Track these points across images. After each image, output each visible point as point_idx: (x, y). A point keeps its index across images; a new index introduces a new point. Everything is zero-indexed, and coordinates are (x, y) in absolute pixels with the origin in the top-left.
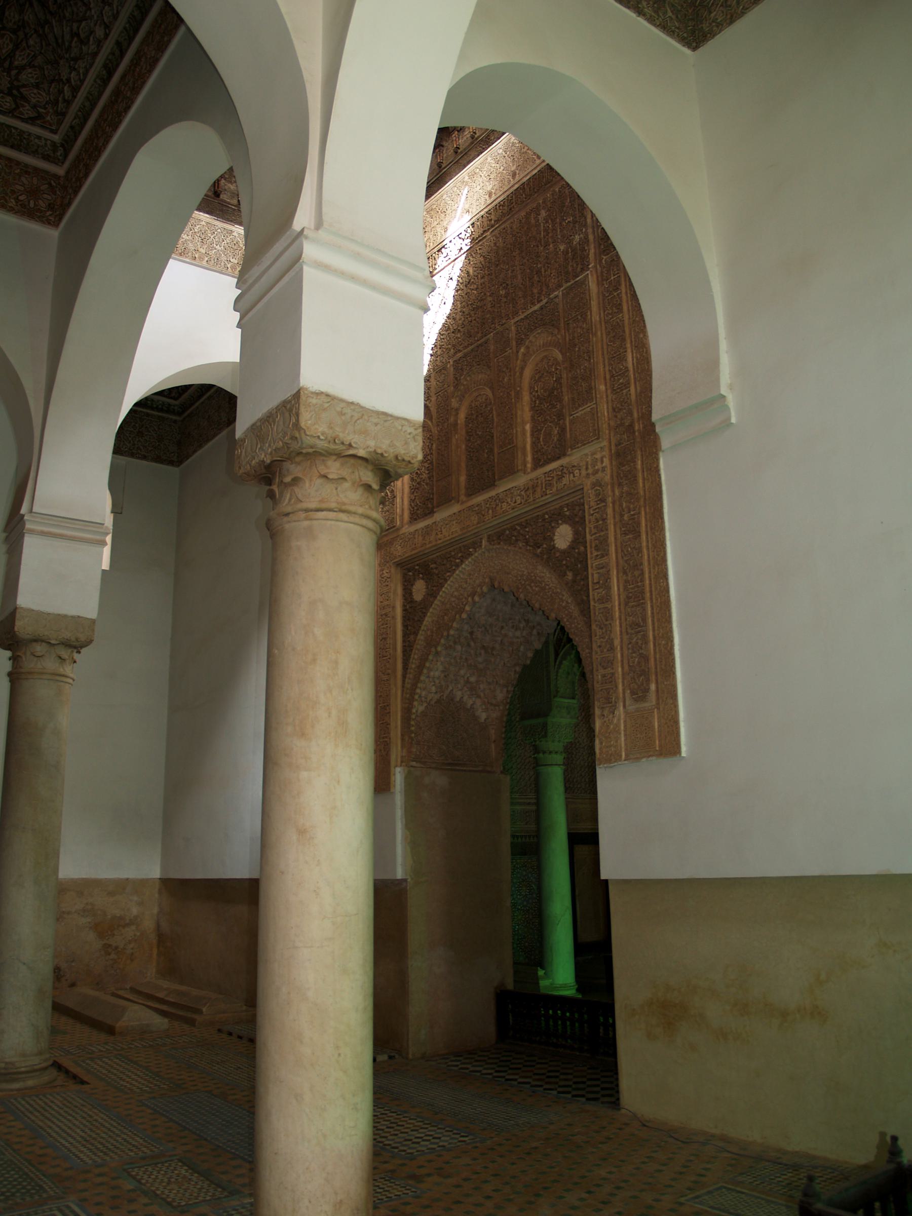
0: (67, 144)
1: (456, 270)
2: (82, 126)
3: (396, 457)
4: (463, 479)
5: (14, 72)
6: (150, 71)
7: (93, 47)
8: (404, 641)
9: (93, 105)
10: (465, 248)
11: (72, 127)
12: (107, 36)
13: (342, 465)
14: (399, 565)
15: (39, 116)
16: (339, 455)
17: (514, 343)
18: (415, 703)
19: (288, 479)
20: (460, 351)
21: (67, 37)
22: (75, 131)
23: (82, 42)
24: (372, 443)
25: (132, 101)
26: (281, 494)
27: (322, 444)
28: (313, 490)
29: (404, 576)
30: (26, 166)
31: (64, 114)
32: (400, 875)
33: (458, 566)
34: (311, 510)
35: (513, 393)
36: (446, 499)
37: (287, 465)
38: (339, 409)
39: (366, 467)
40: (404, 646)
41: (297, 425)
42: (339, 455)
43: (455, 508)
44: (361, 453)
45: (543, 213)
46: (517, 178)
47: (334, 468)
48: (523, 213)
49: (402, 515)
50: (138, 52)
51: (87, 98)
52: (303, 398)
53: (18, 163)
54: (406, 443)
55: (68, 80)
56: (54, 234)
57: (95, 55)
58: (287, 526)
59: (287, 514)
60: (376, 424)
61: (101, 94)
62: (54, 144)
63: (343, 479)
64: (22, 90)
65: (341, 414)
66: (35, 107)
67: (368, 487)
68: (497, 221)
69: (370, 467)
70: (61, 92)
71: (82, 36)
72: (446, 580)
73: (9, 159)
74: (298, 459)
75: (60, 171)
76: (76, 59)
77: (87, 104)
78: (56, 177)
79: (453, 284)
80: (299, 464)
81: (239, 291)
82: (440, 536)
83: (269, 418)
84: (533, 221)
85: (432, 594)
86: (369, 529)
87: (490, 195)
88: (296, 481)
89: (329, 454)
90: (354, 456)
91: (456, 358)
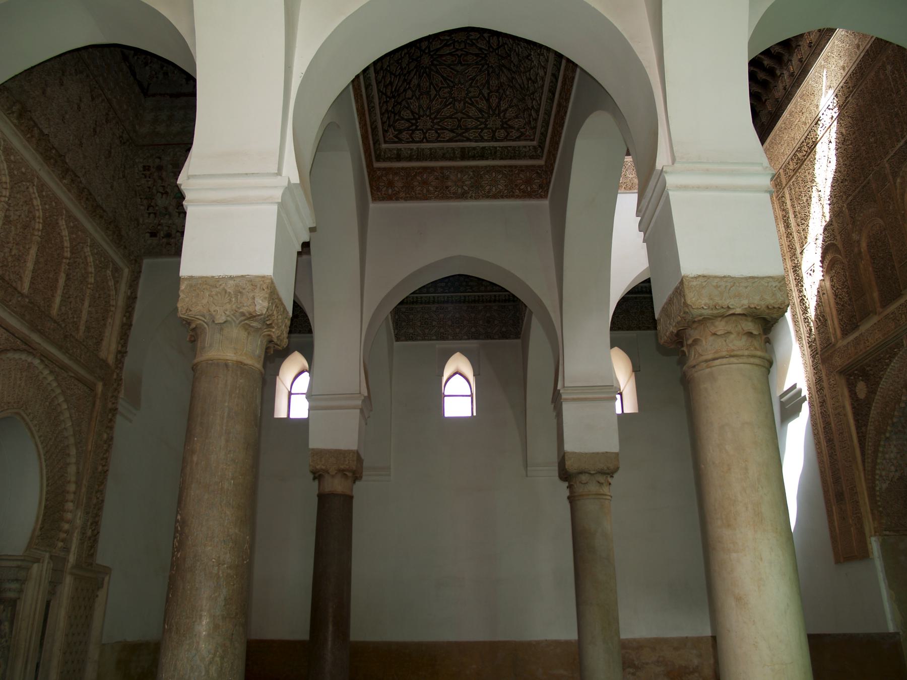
0: (541, 145)
1: (833, 134)
2: (547, 131)
3: (768, 307)
4: (876, 295)
5: (502, 115)
6: (572, 86)
7: (540, 82)
8: (858, 433)
9: (549, 116)
10: (835, 116)
11: (542, 134)
12: (545, 73)
13: (727, 322)
14: (841, 372)
15: (522, 134)
16: (723, 316)
17: (891, 177)
18: (877, 482)
19: (690, 342)
20: (850, 195)
21: (525, 83)
22: (544, 134)
23: (534, 82)
24: (745, 302)
25: (567, 107)
26: (689, 352)
27: (707, 312)
28: (708, 346)
29: (848, 380)
30: (521, 167)
31: (535, 128)
32: (891, 628)
33: (888, 365)
34: (710, 360)
35: (899, 217)
36: (865, 314)
37: (690, 332)
38: (714, 284)
39: (746, 320)
40: (859, 437)
41: (685, 303)
42: (723, 316)
43: (875, 319)
44: (739, 311)
45: (889, 67)
46: (861, 48)
47: (721, 326)
48: (873, 74)
49: (835, 334)
50: (564, 75)
51: (545, 113)
52: (686, 283)
53: (516, 167)
54: (774, 294)
55: (533, 107)
56: (545, 203)
57: (543, 86)
58: (696, 375)
59: (694, 367)
60: (746, 287)
61: (551, 108)
62: (534, 147)
63: (729, 333)
64: (509, 123)
65: (717, 287)
66: (518, 130)
67: (750, 334)
68: (854, 87)
69: (750, 319)
70: (530, 115)
71: (533, 78)
72: (881, 378)
73: (511, 167)
74: (695, 325)
75: (541, 162)
76: (533, 93)
77: (546, 117)
78: (540, 167)
79: (833, 146)
80: (696, 329)
81: (639, 218)
82: (867, 344)
83: (670, 301)
84: (882, 77)
85: (872, 392)
86: (757, 365)
87: (844, 68)
88: (696, 341)
89: (715, 317)
90: (733, 314)
91: (848, 202)
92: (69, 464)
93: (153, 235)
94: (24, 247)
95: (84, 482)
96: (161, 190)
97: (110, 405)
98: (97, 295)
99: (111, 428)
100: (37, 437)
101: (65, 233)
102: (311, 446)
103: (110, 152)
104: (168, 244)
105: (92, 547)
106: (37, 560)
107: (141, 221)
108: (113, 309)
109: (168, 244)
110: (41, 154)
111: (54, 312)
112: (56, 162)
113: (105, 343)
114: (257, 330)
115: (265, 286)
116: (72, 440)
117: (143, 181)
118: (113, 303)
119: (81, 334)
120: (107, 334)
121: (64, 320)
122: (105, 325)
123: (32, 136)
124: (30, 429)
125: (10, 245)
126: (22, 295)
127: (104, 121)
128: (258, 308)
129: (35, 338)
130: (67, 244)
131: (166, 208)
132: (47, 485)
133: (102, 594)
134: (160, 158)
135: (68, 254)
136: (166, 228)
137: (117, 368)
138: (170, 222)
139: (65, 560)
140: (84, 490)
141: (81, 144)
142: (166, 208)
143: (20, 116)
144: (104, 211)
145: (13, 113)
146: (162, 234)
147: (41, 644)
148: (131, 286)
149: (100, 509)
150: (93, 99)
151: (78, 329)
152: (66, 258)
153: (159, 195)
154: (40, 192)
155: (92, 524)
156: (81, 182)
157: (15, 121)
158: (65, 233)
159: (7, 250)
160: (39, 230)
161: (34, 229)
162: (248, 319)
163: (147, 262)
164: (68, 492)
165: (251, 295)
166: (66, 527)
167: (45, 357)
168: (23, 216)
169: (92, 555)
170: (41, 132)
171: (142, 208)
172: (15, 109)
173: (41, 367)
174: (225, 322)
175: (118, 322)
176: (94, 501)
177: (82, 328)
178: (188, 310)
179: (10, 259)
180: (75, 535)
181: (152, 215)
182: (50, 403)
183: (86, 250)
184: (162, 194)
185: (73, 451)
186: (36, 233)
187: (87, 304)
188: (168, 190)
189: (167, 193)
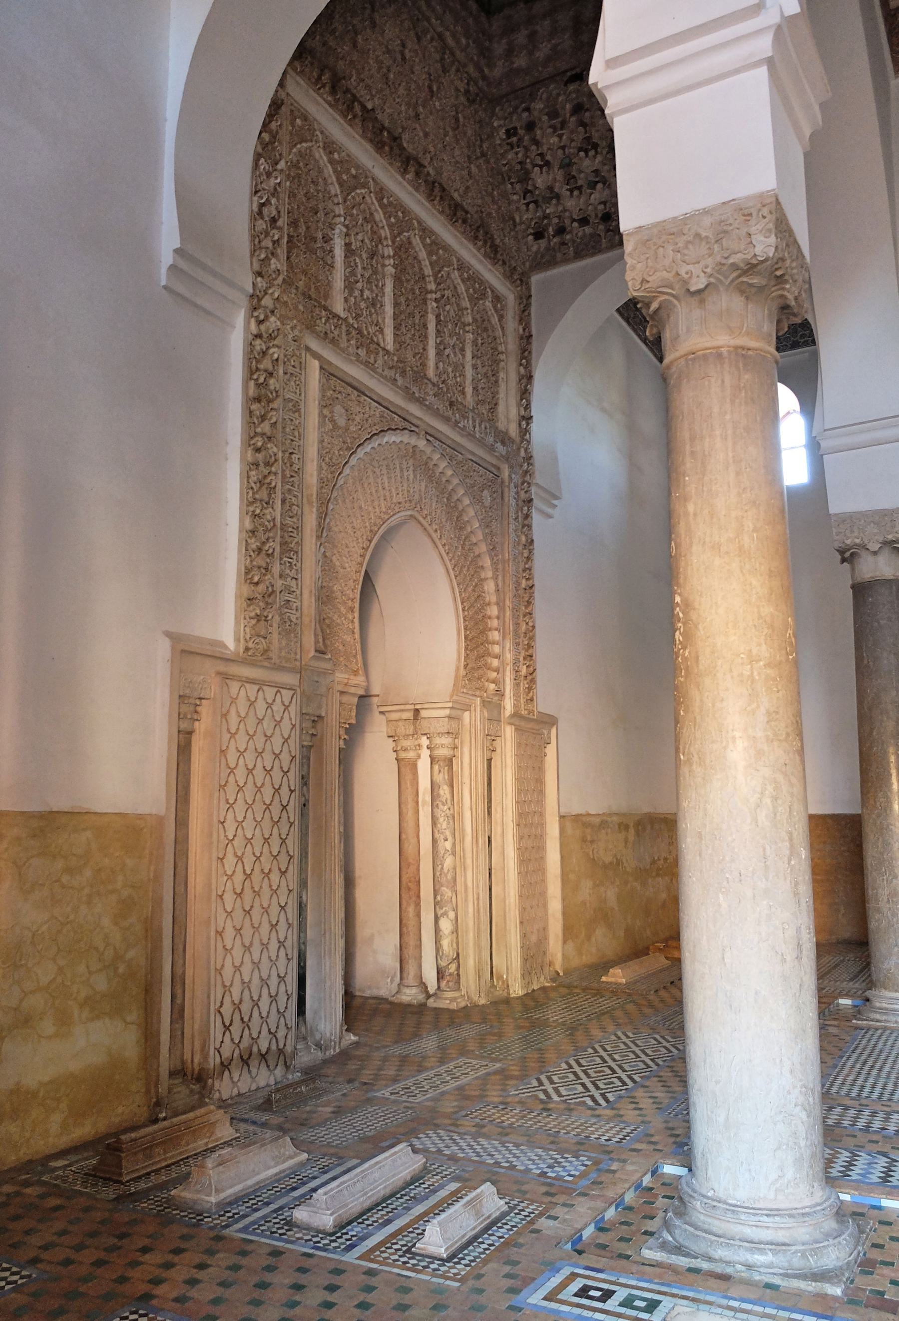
92: (482, 580)
94: (377, 286)
95: (508, 603)
97: (523, 495)
98: (480, 341)
99: (530, 527)
100: (440, 547)
101: (423, 255)
102: (833, 510)
103: (457, 120)
104: (564, 244)
105: (530, 689)
106: (467, 708)
107: (518, 220)
108: (502, 357)
109: (564, 244)
110: (371, 141)
111: (431, 373)
112: (391, 148)
113: (501, 408)
114: (761, 289)
115: (765, 212)
116: (483, 548)
118: (501, 348)
119: (469, 399)
120: (502, 395)
121: (443, 382)
122: (497, 382)
123: (355, 117)
124: (430, 536)
125: (359, 285)
126: (388, 352)
127: (440, 72)
128: (759, 250)
129: (414, 410)
130: (428, 271)
131: (550, 188)
132: (463, 610)
133: (551, 750)
134: (527, 109)
135: (432, 286)
136: (555, 221)
137: (522, 440)
138: (560, 208)
139: (499, 707)
140: (508, 613)
141: (417, 116)
142: (550, 188)
143: (333, 90)
144: (467, 212)
145: (324, 86)
147: (489, 813)
148: (521, 320)
149: (532, 638)
150: (419, 39)
151: (463, 393)
152: (431, 292)
154: (380, 200)
155: (525, 659)
156: (428, 173)
157: (329, 98)
158: (423, 255)
159: (357, 293)
160: (389, 257)
161: (383, 257)
162: (745, 273)
163: (536, 279)
164: (490, 618)
165: (744, 231)
166: (495, 663)
167: (431, 436)
168: (366, 241)
169: (532, 700)
170: (364, 107)
171: (515, 197)
172: (325, 78)
173: (428, 450)
174: (706, 287)
175: (513, 377)
176: (524, 627)
177: (469, 390)
178: (644, 281)
179: (363, 305)
180: (508, 673)
181: (532, 206)
182: (448, 499)
183: (453, 276)
184: (541, 167)
185: (487, 562)
186: (387, 262)
187: (469, 355)
188: (548, 158)
189: (547, 164)
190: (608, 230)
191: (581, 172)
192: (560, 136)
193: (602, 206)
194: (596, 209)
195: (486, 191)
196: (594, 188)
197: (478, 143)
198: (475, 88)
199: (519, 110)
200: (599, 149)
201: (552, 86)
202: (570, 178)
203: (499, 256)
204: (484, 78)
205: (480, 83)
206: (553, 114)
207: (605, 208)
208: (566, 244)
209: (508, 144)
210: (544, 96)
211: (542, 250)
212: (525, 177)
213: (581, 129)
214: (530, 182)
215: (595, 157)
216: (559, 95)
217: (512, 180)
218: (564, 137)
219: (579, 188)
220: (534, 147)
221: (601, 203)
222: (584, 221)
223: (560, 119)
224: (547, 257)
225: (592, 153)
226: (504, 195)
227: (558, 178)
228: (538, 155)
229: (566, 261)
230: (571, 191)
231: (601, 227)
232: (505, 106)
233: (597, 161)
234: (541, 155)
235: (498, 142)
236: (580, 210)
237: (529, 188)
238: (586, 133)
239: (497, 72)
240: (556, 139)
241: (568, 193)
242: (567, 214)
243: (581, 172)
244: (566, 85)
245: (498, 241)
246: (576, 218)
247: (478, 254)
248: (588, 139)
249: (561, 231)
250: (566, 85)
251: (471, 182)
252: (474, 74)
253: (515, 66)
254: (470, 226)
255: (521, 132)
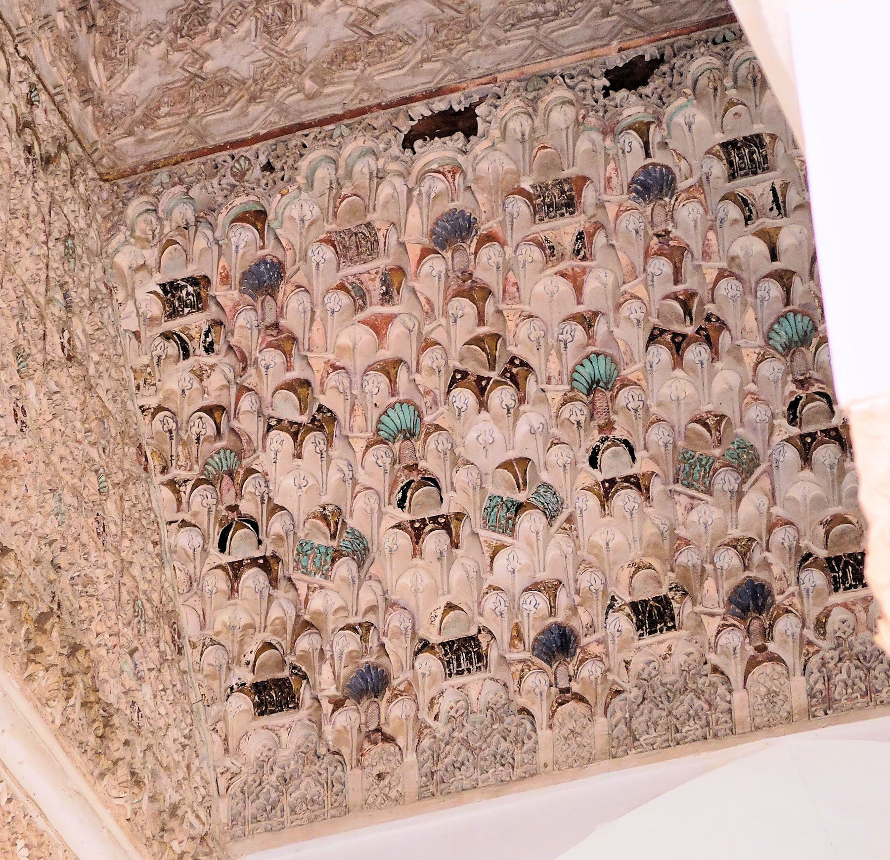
93: (273, 695)
96: (287, 408)
107: (190, 626)
109: (380, 735)
117: (176, 378)
131: (332, 519)
134: (257, 218)
136: (350, 642)
138: (367, 597)
142: (332, 519)
146: (326, 682)
153: (281, 440)
171: (186, 539)
181: (253, 578)
184: (296, 432)
188: (330, 400)
189: (324, 421)
190: (565, 695)
191: (457, 462)
192: (379, 327)
193: (541, 600)
194: (514, 608)
195: (76, 493)
196: (510, 529)
197: (57, 310)
198: (55, 118)
199: (223, 218)
200: (531, 387)
201: (351, 148)
202: (413, 482)
203: (116, 747)
204: (88, 96)
205: (74, 106)
206: (354, 243)
207: (552, 610)
208: (388, 739)
209: (167, 336)
210: (324, 173)
211: (284, 754)
212: (232, 469)
213: (465, 306)
214: (250, 485)
215: (513, 412)
216: (379, 177)
217: (175, 473)
218: (395, 331)
219: (445, 524)
220: (274, 357)
221: (535, 587)
222: (464, 653)
223: (382, 263)
224: (307, 787)
225: (502, 396)
226: (143, 524)
227: (363, 478)
228: (290, 386)
229: (387, 800)
230: (417, 532)
231: (537, 681)
232: (164, 202)
233: (523, 427)
234: (300, 387)
235: (132, 324)
236: (450, 607)
237: (247, 507)
238: (481, 321)
239: (141, 79)
240: (365, 335)
241: (404, 539)
242: (396, 620)
243: (457, 462)
244: (408, 143)
245: (111, 693)
246: (435, 639)
247: (33, 718)
248: (487, 343)
249: (371, 684)
250: (408, 143)
251: (21, 445)
252: (57, 74)
253: (209, 66)
254: (14, 604)
255: (226, 295)
